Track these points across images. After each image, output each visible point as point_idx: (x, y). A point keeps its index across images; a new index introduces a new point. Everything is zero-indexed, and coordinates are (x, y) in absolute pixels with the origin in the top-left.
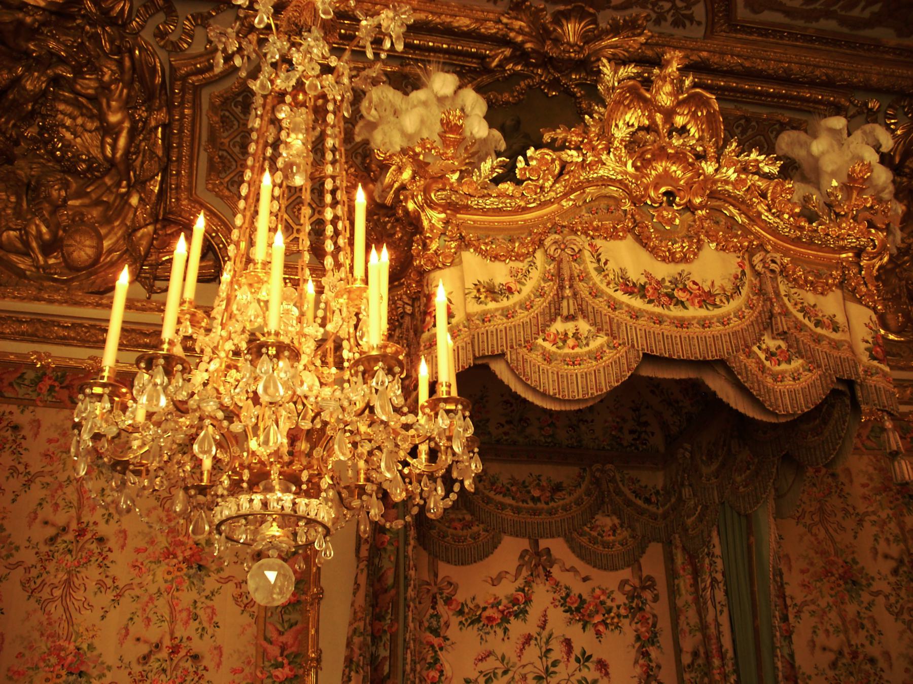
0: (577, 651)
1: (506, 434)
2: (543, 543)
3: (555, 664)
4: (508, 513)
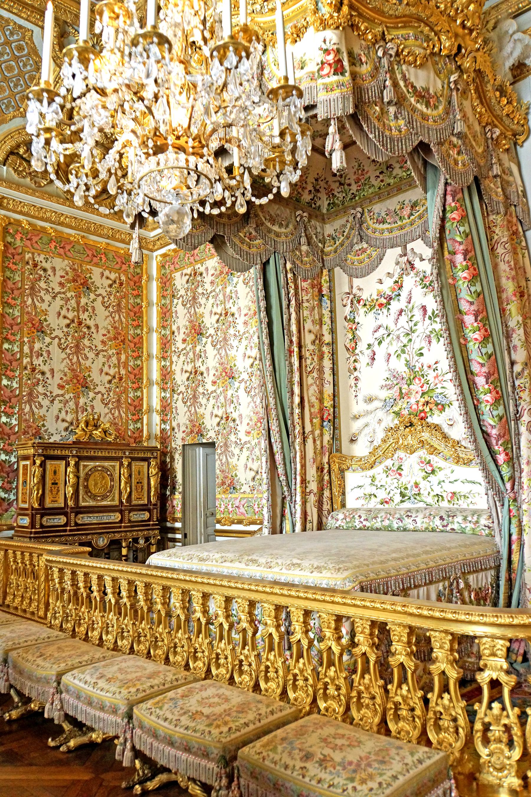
0: (429, 313)
1: (382, 181)
2: (409, 246)
3: (415, 325)
4: (386, 234)
